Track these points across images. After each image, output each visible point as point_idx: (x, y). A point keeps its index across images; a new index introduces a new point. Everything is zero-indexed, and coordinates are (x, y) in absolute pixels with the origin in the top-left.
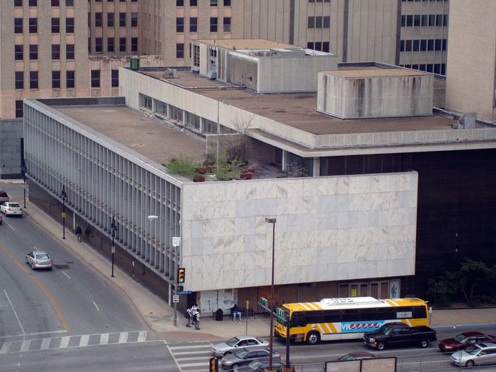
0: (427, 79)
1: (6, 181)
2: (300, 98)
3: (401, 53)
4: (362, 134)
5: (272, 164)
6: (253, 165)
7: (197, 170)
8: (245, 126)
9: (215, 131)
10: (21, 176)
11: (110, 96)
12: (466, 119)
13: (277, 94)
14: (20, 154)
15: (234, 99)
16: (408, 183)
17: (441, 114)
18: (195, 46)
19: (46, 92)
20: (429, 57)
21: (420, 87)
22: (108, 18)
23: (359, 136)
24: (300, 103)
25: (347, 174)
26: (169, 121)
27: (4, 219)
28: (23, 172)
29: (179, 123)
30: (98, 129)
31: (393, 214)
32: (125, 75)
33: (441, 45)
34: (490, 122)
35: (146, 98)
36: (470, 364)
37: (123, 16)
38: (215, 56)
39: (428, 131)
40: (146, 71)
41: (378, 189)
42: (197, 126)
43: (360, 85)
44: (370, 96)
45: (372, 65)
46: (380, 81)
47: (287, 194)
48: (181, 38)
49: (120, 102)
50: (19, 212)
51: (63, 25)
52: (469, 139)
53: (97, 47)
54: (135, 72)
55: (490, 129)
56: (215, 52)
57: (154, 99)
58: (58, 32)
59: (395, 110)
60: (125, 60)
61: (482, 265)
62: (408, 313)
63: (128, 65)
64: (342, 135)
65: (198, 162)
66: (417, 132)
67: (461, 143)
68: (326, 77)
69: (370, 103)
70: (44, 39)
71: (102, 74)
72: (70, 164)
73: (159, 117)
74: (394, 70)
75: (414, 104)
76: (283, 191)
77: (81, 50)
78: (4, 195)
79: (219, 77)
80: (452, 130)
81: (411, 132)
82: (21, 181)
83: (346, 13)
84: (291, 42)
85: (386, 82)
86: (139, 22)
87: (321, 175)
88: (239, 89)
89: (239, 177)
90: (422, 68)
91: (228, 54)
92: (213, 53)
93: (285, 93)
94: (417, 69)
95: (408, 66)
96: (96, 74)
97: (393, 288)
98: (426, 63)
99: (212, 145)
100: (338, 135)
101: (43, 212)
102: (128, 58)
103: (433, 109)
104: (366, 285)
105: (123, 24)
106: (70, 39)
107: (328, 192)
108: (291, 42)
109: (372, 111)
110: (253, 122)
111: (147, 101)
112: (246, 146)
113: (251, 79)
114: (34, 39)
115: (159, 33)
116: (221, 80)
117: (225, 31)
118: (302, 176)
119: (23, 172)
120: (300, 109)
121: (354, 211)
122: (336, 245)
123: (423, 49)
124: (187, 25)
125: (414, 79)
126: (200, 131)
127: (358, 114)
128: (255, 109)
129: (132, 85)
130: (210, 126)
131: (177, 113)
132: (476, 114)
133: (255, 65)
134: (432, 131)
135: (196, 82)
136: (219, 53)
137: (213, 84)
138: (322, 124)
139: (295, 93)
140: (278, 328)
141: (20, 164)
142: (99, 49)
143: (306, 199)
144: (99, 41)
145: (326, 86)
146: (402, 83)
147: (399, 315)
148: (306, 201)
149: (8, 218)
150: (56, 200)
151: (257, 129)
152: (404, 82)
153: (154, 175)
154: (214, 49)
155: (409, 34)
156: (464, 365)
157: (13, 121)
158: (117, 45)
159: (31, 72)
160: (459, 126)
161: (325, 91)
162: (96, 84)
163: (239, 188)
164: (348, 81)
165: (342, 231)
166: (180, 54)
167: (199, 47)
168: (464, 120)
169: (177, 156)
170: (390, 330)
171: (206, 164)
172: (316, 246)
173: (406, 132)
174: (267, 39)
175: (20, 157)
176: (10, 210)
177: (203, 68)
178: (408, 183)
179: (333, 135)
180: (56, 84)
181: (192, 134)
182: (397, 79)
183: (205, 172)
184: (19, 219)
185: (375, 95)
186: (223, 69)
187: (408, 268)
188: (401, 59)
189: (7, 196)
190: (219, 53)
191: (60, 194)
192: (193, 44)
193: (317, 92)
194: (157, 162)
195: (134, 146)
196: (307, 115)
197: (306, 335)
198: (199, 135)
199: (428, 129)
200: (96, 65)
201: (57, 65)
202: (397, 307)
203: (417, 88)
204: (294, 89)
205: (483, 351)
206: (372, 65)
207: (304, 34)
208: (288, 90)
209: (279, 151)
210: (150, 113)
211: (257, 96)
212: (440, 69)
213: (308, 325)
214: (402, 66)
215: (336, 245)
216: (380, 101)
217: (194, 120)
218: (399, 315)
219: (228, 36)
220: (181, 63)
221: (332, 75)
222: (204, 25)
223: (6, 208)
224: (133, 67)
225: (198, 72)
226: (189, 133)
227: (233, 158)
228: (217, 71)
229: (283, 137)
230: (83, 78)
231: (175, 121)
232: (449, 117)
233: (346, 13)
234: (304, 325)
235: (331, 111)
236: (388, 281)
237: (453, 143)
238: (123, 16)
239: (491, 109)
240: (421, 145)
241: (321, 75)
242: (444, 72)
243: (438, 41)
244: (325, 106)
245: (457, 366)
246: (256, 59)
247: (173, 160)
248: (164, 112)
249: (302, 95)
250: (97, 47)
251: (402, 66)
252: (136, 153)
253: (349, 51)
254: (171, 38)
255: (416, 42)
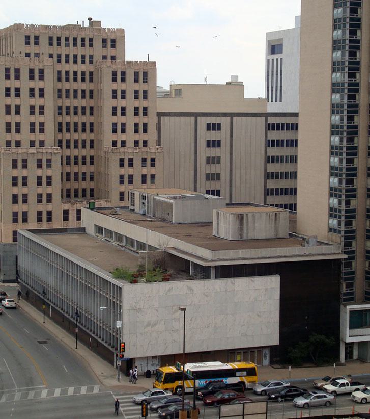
0: (284, 214)
1: (6, 285)
2: (202, 226)
3: (268, 197)
4: (242, 250)
5: (183, 271)
6: (171, 272)
7: (133, 276)
8: (165, 246)
9: (145, 249)
10: (16, 281)
11: (76, 227)
12: (310, 240)
13: (186, 224)
14: (15, 266)
15: (157, 227)
16: (273, 282)
17: (294, 237)
18: (132, 193)
19: (33, 224)
20: (285, 199)
21: (280, 219)
22: (75, 176)
23: (240, 251)
24: (201, 230)
25: (233, 277)
26: (114, 243)
27: (4, 310)
28: (17, 279)
29: (121, 244)
30: (67, 249)
31: (264, 303)
32: (85, 213)
33: (293, 191)
34: (326, 242)
35: (99, 228)
36: (306, 406)
37: (84, 174)
38: (145, 199)
39: (285, 248)
40: (99, 210)
41: (254, 287)
42: (133, 246)
43: (241, 217)
44: (247, 225)
45: (248, 204)
46: (254, 215)
47: (193, 291)
48: (122, 188)
49: (82, 231)
50: (14, 306)
51: (44, 181)
52: (313, 253)
53: (67, 195)
54: (92, 211)
55: (326, 246)
56: (145, 197)
57: (105, 229)
58: (41, 185)
59: (264, 234)
60: (85, 203)
61: (323, 337)
62: (243, 372)
63: (88, 206)
64: (230, 251)
65: (133, 270)
66: (279, 248)
67: (307, 256)
68: (218, 212)
69: (247, 230)
70: (32, 190)
71: (70, 212)
72: (48, 272)
73: (108, 240)
74: (263, 208)
75: (276, 230)
76: (190, 289)
77: (57, 197)
78: (4, 294)
79: (148, 213)
80: (301, 247)
81: (274, 249)
82: (16, 285)
83: (231, 171)
84: (195, 190)
85: (258, 215)
86: (95, 178)
87: (216, 278)
88: (161, 221)
89: (161, 280)
90: (281, 206)
91: (153, 198)
92: (144, 197)
93: (191, 223)
94: (278, 207)
95: (272, 205)
96: (66, 213)
97: (265, 354)
98: (284, 203)
99: (143, 258)
100: (227, 251)
101: (31, 305)
102: (87, 202)
103: (289, 234)
104: (247, 352)
105: (84, 179)
106: (49, 190)
107: (221, 289)
108: (195, 190)
109: (249, 235)
110: (169, 243)
111: (99, 230)
112: (166, 259)
113: (169, 214)
114: (25, 190)
115: (108, 185)
116: (149, 215)
117: (151, 183)
118: (204, 279)
119: (17, 279)
120: (201, 234)
121: (238, 302)
122: (227, 325)
123: (282, 194)
124: (126, 180)
125: (276, 214)
126: (135, 249)
127: (239, 236)
128: (171, 234)
129: (90, 219)
130: (141, 246)
131: (119, 237)
132: (316, 236)
133: (172, 205)
134: (288, 248)
135: (133, 217)
136: (148, 197)
137: (143, 218)
138: (216, 243)
139: (198, 223)
140: (156, 384)
141: (15, 273)
142: (68, 196)
143: (206, 294)
144: (68, 191)
145: (218, 219)
146: (268, 217)
147: (238, 374)
148: (206, 296)
149: (7, 310)
150: (39, 297)
151: (173, 247)
152: (270, 216)
153: (104, 279)
154: (144, 195)
155: (272, 184)
156: (302, 406)
157: (11, 245)
158: (80, 193)
159: (23, 212)
160: (306, 244)
161: (218, 221)
162: (66, 218)
163: (161, 288)
164: (233, 215)
165: (231, 315)
166: (122, 199)
167: (134, 194)
168: (309, 241)
169: (119, 266)
170: (213, 386)
171: (139, 271)
172: (213, 326)
173: (271, 249)
174: (179, 188)
175: (15, 268)
176: (8, 304)
177: (137, 208)
178: (273, 282)
179: (224, 251)
180: (40, 220)
181: (129, 251)
182: (264, 214)
183: (138, 277)
184: (14, 310)
185: (250, 225)
186: (150, 207)
187: (273, 338)
188: (267, 200)
189: (6, 295)
190: (148, 197)
191: (41, 293)
192: (130, 192)
193: (212, 223)
194: (106, 270)
195: (91, 260)
196: (205, 238)
197: (174, 389)
198: (134, 251)
199: (286, 247)
200: (66, 207)
201: (40, 207)
202: (237, 369)
203: (278, 219)
204: (198, 221)
205: (315, 397)
206: (248, 204)
207: (204, 185)
208: (193, 221)
209: (188, 262)
210: (102, 237)
211: (173, 225)
212: (292, 207)
213: (176, 382)
214: (268, 205)
215: (227, 325)
216: (254, 229)
217: (131, 241)
218: (238, 374)
219: (154, 186)
220: (122, 204)
221: (223, 211)
222: (138, 179)
223: (5, 303)
224: (91, 208)
225: (134, 210)
226: (127, 251)
227: (157, 267)
228: (146, 209)
229: (191, 252)
230: (58, 216)
231: (118, 243)
232: (299, 239)
233: (231, 171)
234: (173, 382)
235: (222, 235)
236: (261, 349)
237: (303, 256)
238: (84, 174)
239: (327, 233)
240: (281, 257)
241: (215, 211)
242: (295, 209)
243: (291, 189)
244: (218, 232)
245: (299, 407)
246: (172, 201)
247: (116, 269)
248: (111, 237)
249: (203, 224)
250: (67, 195)
251: (268, 205)
252: (92, 264)
253: (233, 196)
254: (116, 188)
255: (277, 189)
